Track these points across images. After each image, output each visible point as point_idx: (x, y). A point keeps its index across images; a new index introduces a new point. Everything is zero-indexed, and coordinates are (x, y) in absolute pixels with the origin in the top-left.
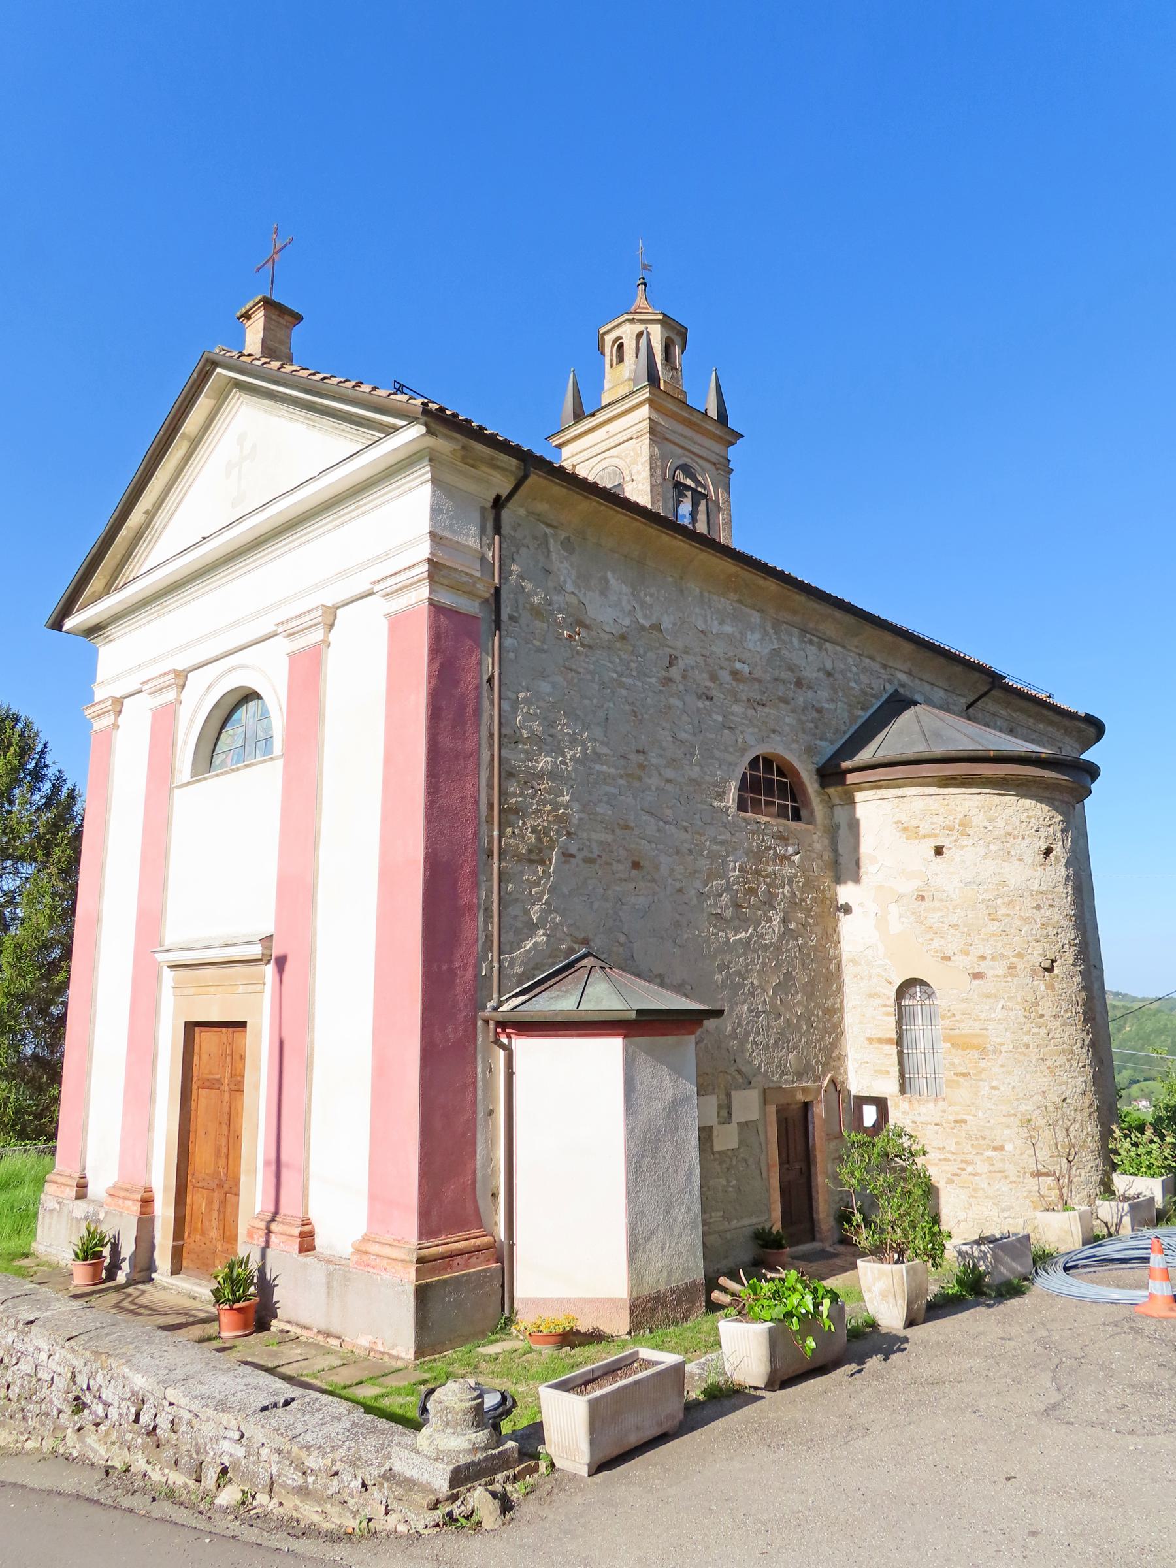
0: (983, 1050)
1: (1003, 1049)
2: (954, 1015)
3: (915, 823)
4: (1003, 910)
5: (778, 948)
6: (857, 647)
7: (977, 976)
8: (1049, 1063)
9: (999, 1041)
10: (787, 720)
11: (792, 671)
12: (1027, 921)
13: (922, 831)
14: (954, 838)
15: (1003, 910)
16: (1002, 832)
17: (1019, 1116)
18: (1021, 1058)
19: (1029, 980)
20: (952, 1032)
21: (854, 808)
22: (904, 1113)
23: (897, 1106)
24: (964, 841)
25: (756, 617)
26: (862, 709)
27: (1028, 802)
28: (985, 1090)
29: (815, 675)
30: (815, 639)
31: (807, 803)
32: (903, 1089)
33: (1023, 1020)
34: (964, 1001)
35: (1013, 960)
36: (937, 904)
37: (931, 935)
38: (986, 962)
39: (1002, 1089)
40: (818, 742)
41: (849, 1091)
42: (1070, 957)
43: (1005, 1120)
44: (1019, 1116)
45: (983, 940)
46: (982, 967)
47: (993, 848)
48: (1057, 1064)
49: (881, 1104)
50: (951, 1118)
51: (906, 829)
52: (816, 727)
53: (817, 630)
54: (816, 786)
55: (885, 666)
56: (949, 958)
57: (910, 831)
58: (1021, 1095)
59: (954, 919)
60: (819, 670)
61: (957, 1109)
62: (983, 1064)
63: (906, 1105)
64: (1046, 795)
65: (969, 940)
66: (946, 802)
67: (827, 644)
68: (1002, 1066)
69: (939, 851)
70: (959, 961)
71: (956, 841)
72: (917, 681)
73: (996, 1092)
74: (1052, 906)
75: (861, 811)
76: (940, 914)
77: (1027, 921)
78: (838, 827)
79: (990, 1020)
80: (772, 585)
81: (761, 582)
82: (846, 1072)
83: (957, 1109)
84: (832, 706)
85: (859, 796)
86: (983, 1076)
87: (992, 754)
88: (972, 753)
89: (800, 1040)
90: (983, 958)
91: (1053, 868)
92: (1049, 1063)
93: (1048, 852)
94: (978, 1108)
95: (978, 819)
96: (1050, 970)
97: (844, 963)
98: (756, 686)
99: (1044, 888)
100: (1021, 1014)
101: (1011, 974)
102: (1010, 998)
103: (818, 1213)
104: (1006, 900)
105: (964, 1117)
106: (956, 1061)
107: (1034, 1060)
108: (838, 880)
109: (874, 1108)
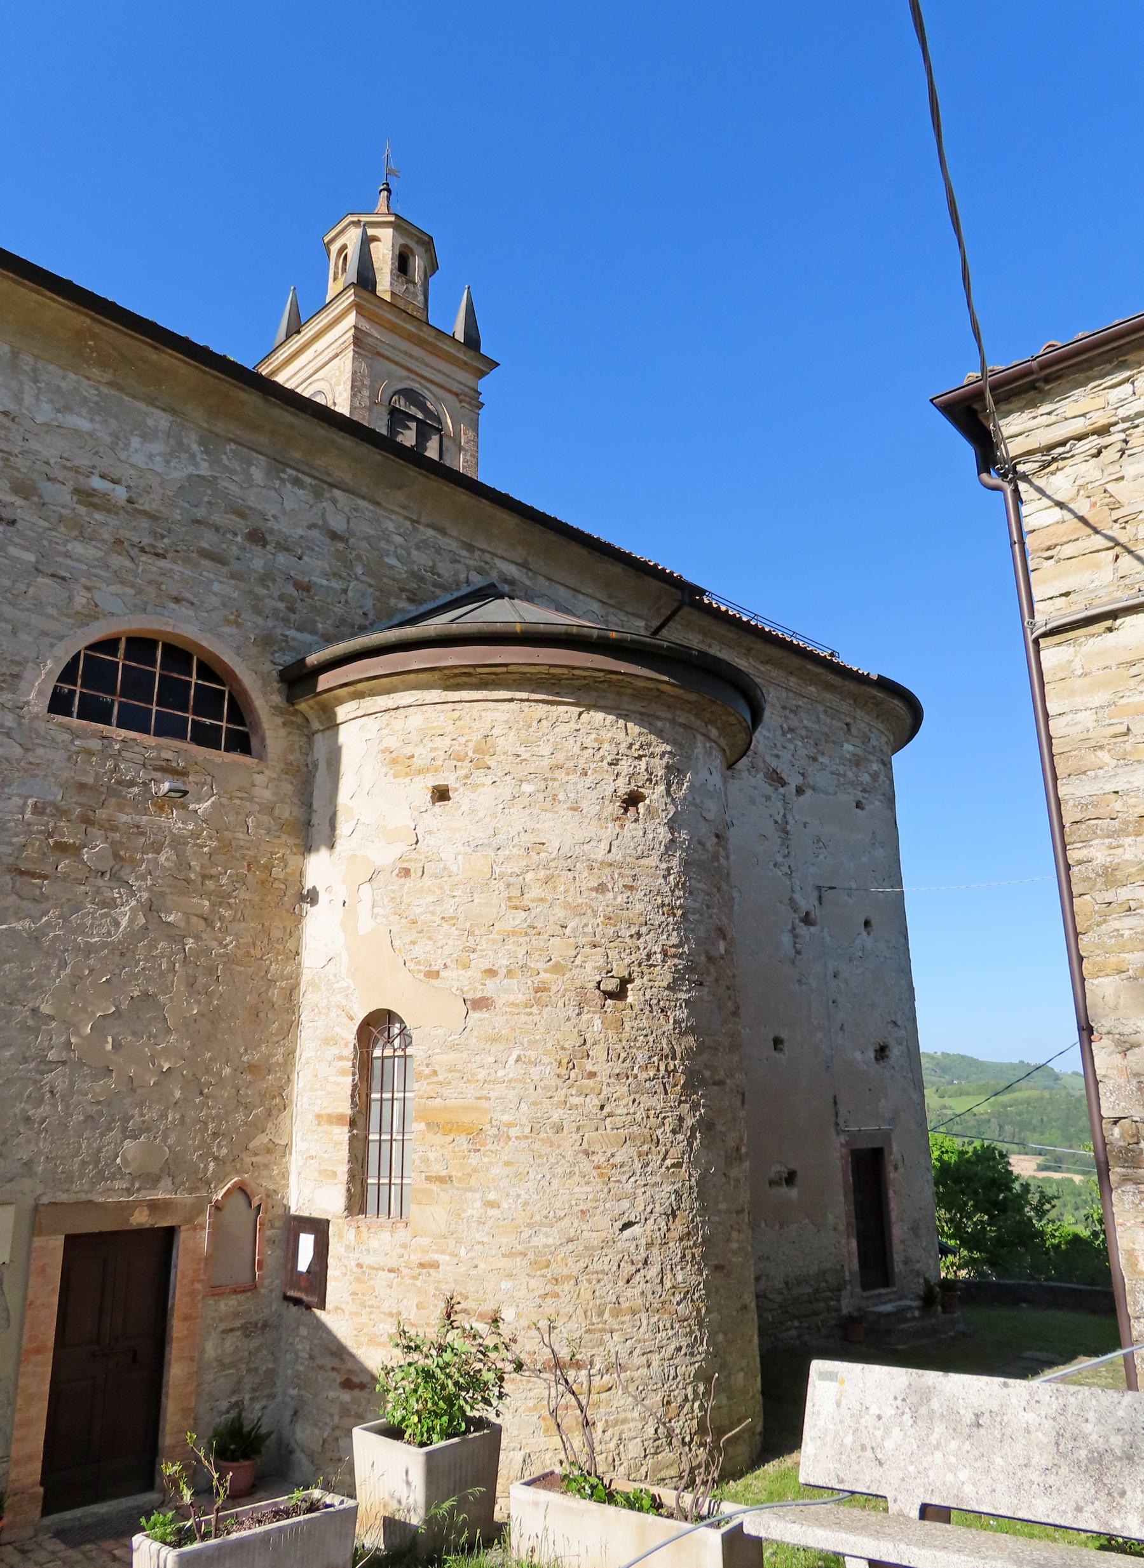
0: (475, 1134)
1: (513, 1132)
2: (435, 1073)
3: (408, 751)
4: (535, 892)
5: (123, 951)
6: (404, 507)
7: (481, 1004)
8: (599, 1159)
9: (506, 1118)
10: (216, 587)
11: (242, 515)
12: (577, 911)
13: (417, 762)
14: (463, 772)
15: (535, 892)
16: (546, 763)
17: (531, 1256)
18: (545, 1149)
19: (572, 1012)
20: (430, 1103)
21: (337, 734)
22: (347, 1247)
23: (340, 1236)
24: (479, 777)
25: (161, 420)
26: (411, 600)
27: (598, 717)
28: (475, 1208)
29: (300, 531)
30: (308, 480)
31: (256, 725)
32: (357, 1203)
33: (554, 1082)
34: (453, 1047)
35: (544, 976)
36: (427, 881)
37: (414, 936)
38: (497, 980)
39: (504, 1205)
40: (291, 633)
41: (287, 1208)
42: (663, 976)
43: (503, 1263)
44: (531, 1256)
45: (494, 941)
46: (490, 988)
47: (527, 788)
48: (617, 1160)
49: (320, 1228)
50: (415, 1258)
51: (394, 761)
52: (292, 609)
53: (312, 467)
54: (277, 699)
55: (470, 548)
56: (436, 974)
57: (399, 764)
58: (537, 1218)
59: (449, 907)
60: (311, 526)
61: (425, 1241)
62: (474, 1160)
63: (351, 1234)
64: (638, 707)
65: (471, 943)
66: (456, 714)
67: (337, 493)
68: (507, 1164)
69: (441, 794)
70: (454, 978)
71: (467, 777)
72: (541, 580)
73: (492, 1212)
74: (631, 888)
75: (347, 736)
76: (431, 899)
77: (577, 911)
78: (316, 766)
79: (494, 1082)
80: (56, 308)
81: (153, 356)
82: (285, 1175)
83: (425, 1241)
84: (336, 584)
85: (343, 712)
86: (473, 1182)
87: (518, 628)
88: (486, 628)
89: (163, 1116)
90: (491, 972)
91: (640, 826)
92: (599, 1159)
93: (633, 800)
94: (458, 1242)
95: (507, 743)
96: (619, 994)
97: (303, 987)
98: (145, 523)
99: (617, 855)
100: (550, 1070)
101: (538, 1002)
102: (533, 1043)
103: (164, 1436)
104: (542, 874)
105: (436, 1257)
106: (432, 1156)
107: (569, 1154)
108: (308, 848)
109: (311, 1237)
